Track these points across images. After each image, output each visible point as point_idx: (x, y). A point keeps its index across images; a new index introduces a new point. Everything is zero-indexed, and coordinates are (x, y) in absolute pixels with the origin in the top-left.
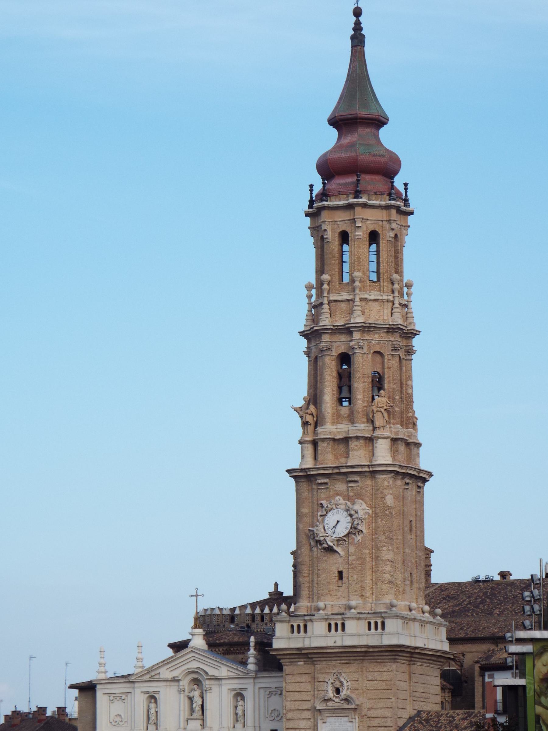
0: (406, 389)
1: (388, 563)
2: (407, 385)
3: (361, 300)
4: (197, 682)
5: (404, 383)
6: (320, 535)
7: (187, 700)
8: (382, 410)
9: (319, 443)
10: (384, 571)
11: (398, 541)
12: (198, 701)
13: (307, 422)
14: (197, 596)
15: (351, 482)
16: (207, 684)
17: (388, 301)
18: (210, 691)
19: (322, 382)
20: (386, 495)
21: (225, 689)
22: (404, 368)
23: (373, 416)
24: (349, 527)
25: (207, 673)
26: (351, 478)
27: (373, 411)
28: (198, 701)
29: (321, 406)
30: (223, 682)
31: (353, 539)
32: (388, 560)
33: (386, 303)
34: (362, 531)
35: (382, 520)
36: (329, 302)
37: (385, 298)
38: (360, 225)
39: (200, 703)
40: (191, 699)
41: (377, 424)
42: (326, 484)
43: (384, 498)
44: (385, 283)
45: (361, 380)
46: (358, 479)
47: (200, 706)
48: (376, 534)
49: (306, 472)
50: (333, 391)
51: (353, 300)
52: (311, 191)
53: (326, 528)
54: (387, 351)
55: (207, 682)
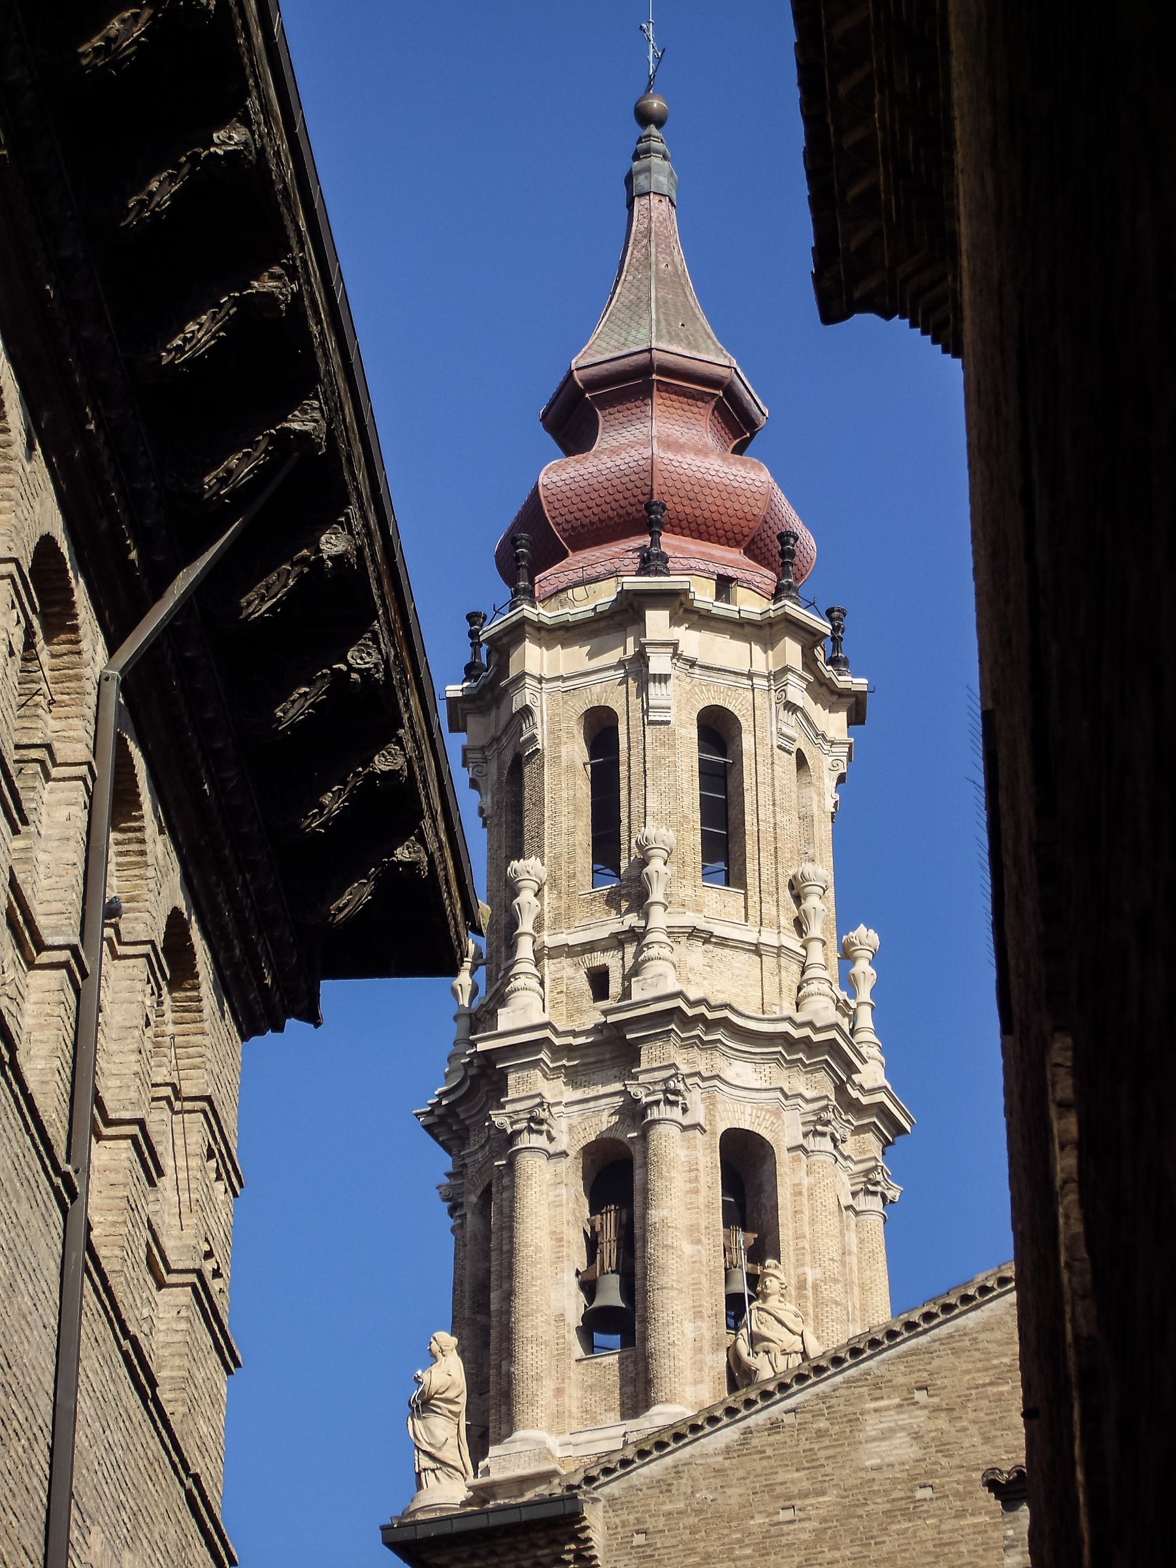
3: (671, 932)
17: (780, 950)
36: (539, 957)
37: (769, 937)
51: (636, 936)
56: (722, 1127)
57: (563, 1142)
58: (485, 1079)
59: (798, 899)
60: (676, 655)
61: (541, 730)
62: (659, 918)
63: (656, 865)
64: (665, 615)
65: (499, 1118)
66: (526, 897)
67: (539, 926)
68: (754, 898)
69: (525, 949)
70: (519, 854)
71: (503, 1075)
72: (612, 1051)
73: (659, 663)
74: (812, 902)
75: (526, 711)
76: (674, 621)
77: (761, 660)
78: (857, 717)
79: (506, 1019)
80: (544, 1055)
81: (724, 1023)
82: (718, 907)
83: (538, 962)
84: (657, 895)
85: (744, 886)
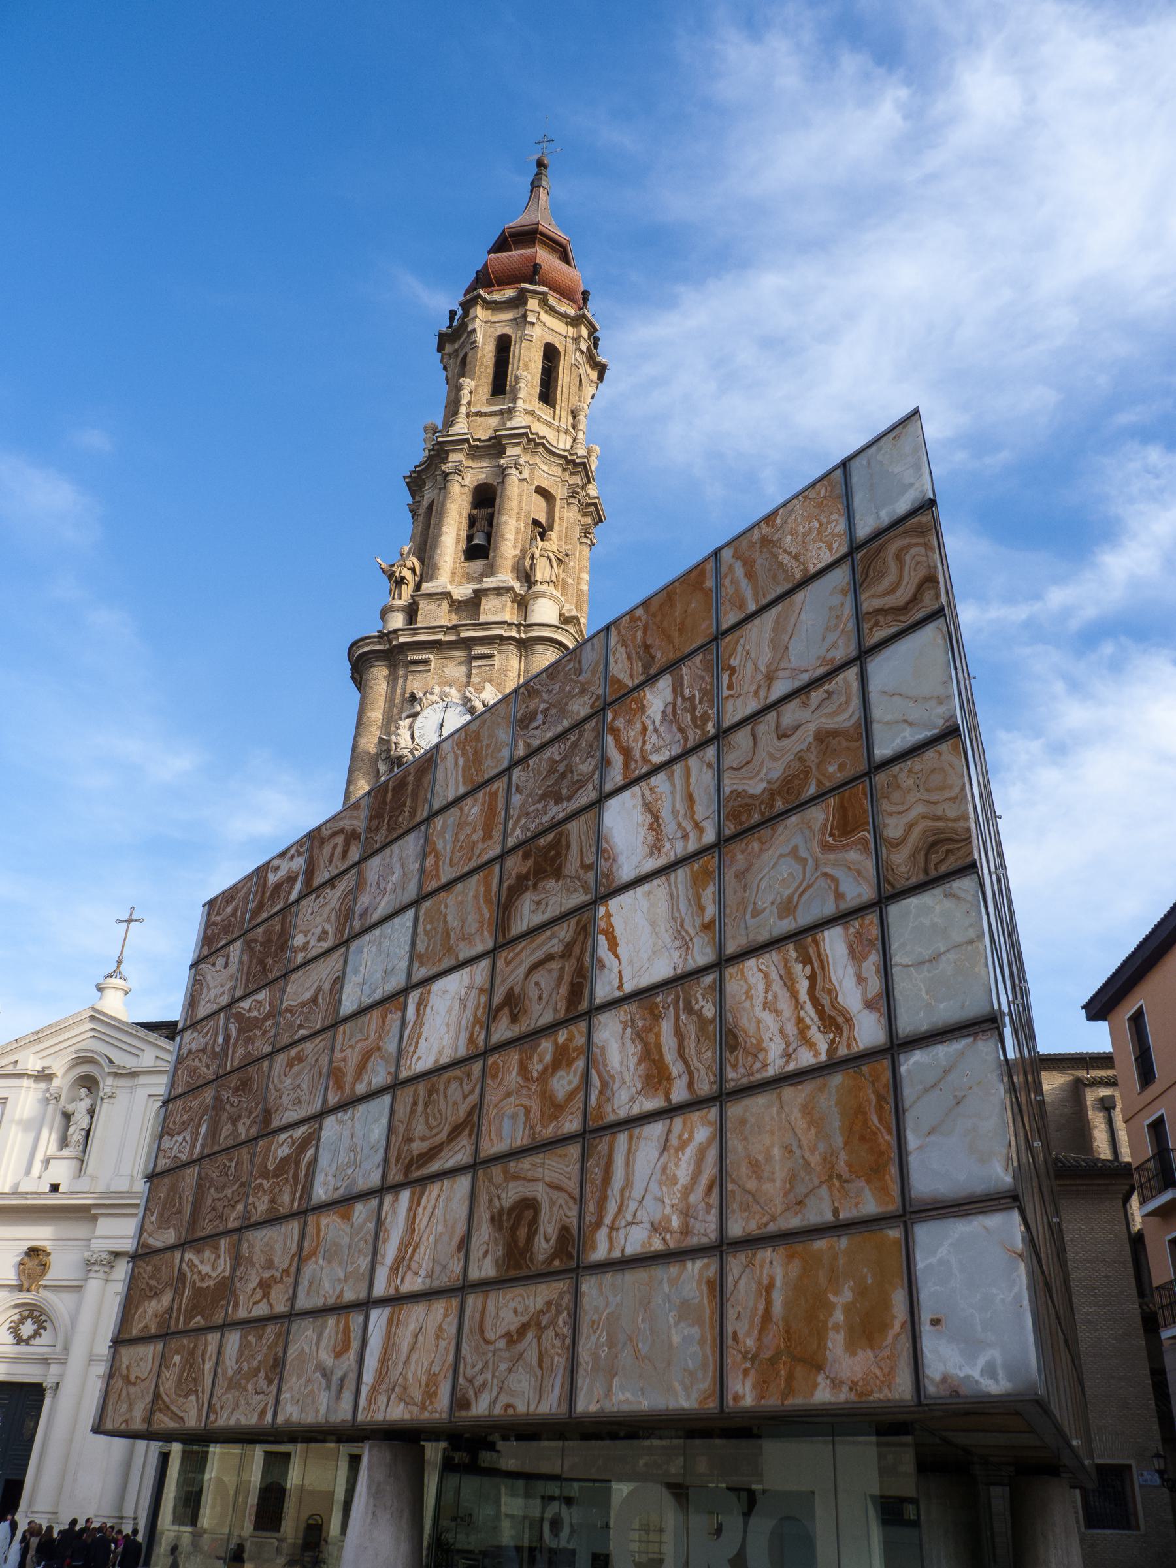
4: (88, 1083)
6: (403, 746)
7: (58, 1118)
8: (552, 557)
9: (422, 605)
12: (81, 1120)
13: (403, 578)
14: (130, 921)
16: (107, 1084)
18: (111, 1100)
19: (439, 526)
21: (141, 1094)
23: (532, 564)
25: (111, 1061)
26: (478, 651)
27: (533, 555)
28: (81, 1120)
29: (431, 557)
30: (142, 1080)
33: (562, 435)
36: (468, 415)
38: (534, 320)
39: (85, 1126)
40: (67, 1116)
41: (539, 577)
44: (564, 414)
45: (514, 515)
47: (83, 1133)
49: (390, 642)
50: (458, 535)
52: (452, 318)
53: (416, 735)
54: (560, 492)
55: (109, 1081)
56: (536, 484)
57: (467, 482)
58: (438, 453)
59: (574, 417)
60: (538, 318)
61: (479, 338)
62: (520, 403)
63: (522, 385)
65: (443, 467)
66: (466, 392)
67: (469, 403)
68: (558, 412)
69: (463, 410)
70: (463, 376)
71: (447, 453)
72: (495, 447)
73: (531, 318)
74: (581, 417)
75: (474, 331)
77: (571, 331)
78: (601, 378)
79: (452, 431)
80: (466, 446)
81: (543, 444)
83: (468, 416)
84: (521, 395)
85: (554, 407)
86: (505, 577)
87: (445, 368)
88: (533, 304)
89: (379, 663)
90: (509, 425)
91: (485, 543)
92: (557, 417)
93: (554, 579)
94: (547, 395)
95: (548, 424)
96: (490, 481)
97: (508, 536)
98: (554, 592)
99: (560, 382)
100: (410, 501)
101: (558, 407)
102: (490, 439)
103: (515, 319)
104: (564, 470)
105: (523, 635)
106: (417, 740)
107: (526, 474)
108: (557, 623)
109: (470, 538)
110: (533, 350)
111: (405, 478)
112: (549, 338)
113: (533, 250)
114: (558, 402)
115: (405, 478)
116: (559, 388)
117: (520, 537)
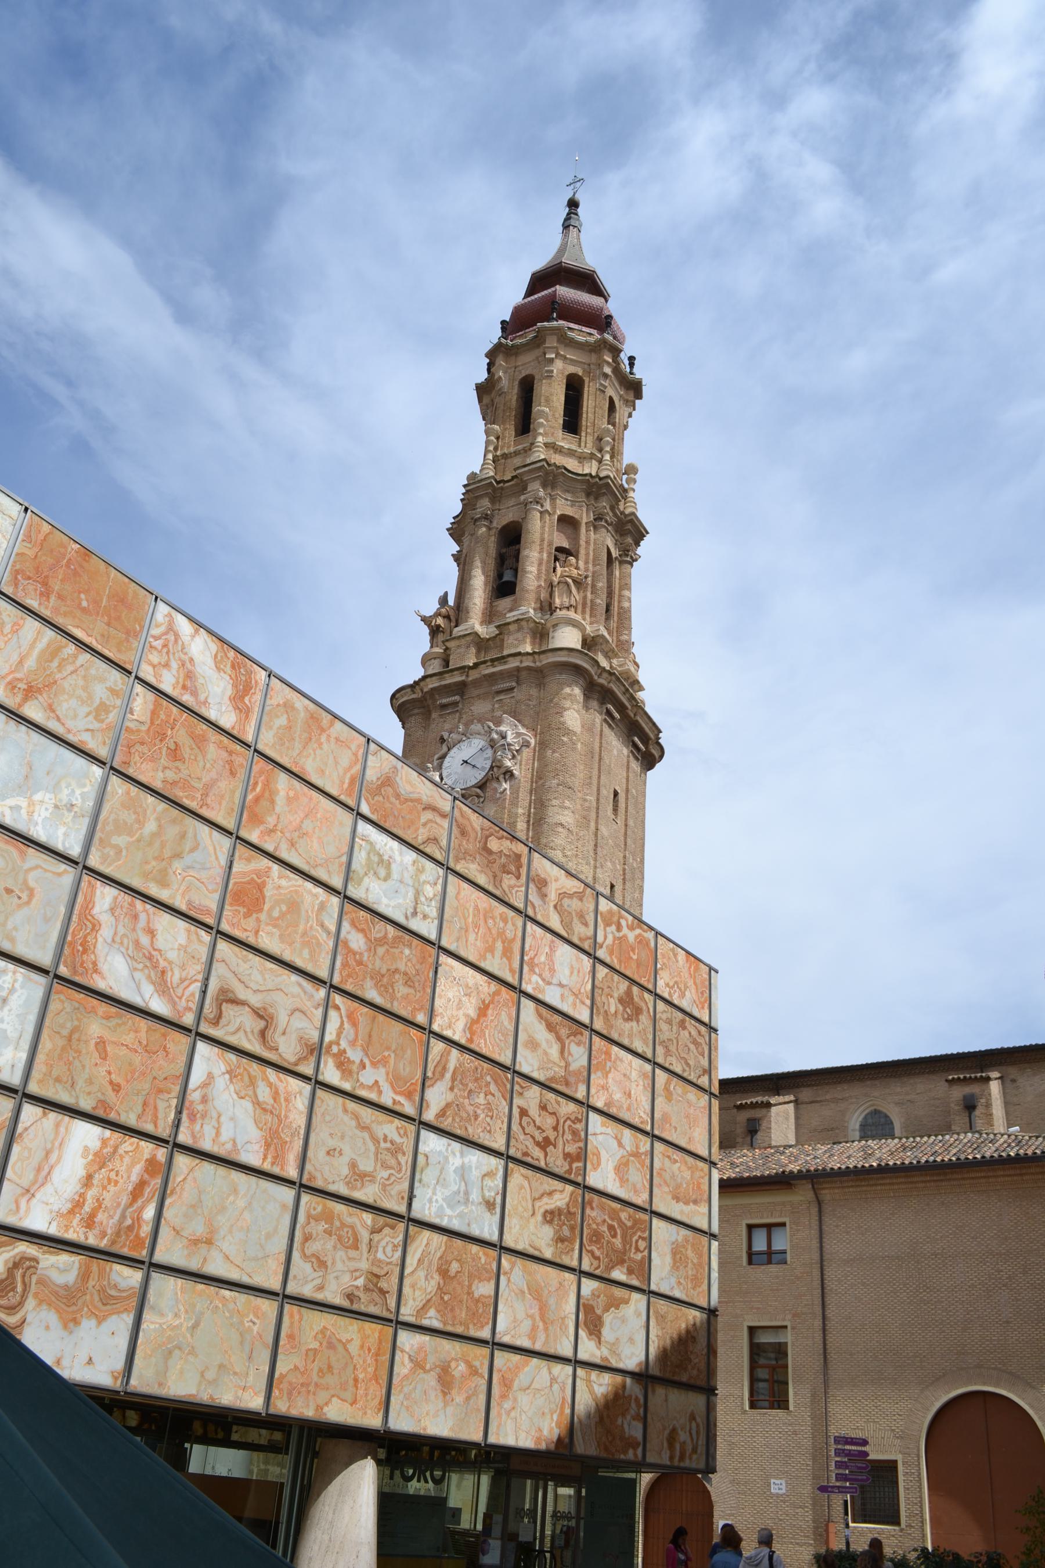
0: (619, 602)
1: (560, 829)
2: (620, 596)
3: (546, 445)
5: (617, 592)
8: (569, 580)
10: (552, 844)
11: (587, 804)
15: (499, 692)
20: (566, 709)
22: (617, 573)
24: (488, 766)
31: (495, 789)
32: (562, 825)
34: (512, 775)
35: (554, 752)
42: (455, 704)
43: (560, 714)
44: (590, 439)
46: (514, 684)
48: (541, 778)
54: (585, 517)
56: (559, 513)
64: (555, 338)
68: (583, 438)
76: (559, 341)
77: (594, 358)
82: (566, 441)
86: (529, 609)
87: (484, 419)
88: (551, 342)
89: (416, 711)
90: (528, 461)
91: (513, 579)
92: (583, 444)
93: (573, 603)
94: (572, 423)
95: (571, 453)
96: (516, 519)
97: (529, 568)
98: (578, 617)
99: (585, 409)
100: (455, 548)
101: (583, 434)
102: (513, 478)
103: (537, 358)
104: (588, 495)
105: (538, 664)
106: (445, 780)
107: (548, 506)
108: (579, 647)
109: (500, 576)
110: (555, 385)
111: (448, 530)
112: (572, 369)
113: (553, 289)
114: (584, 428)
115: (448, 530)
116: (584, 415)
117: (544, 568)
